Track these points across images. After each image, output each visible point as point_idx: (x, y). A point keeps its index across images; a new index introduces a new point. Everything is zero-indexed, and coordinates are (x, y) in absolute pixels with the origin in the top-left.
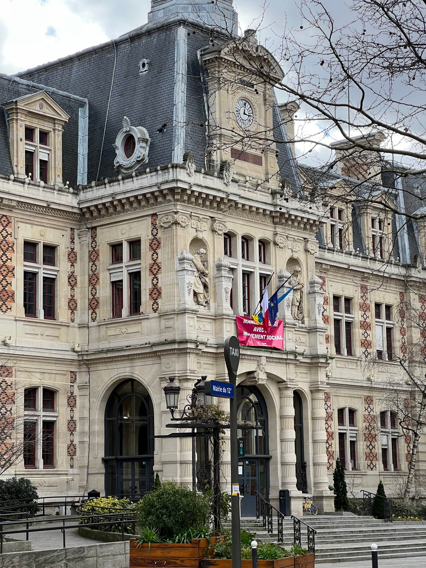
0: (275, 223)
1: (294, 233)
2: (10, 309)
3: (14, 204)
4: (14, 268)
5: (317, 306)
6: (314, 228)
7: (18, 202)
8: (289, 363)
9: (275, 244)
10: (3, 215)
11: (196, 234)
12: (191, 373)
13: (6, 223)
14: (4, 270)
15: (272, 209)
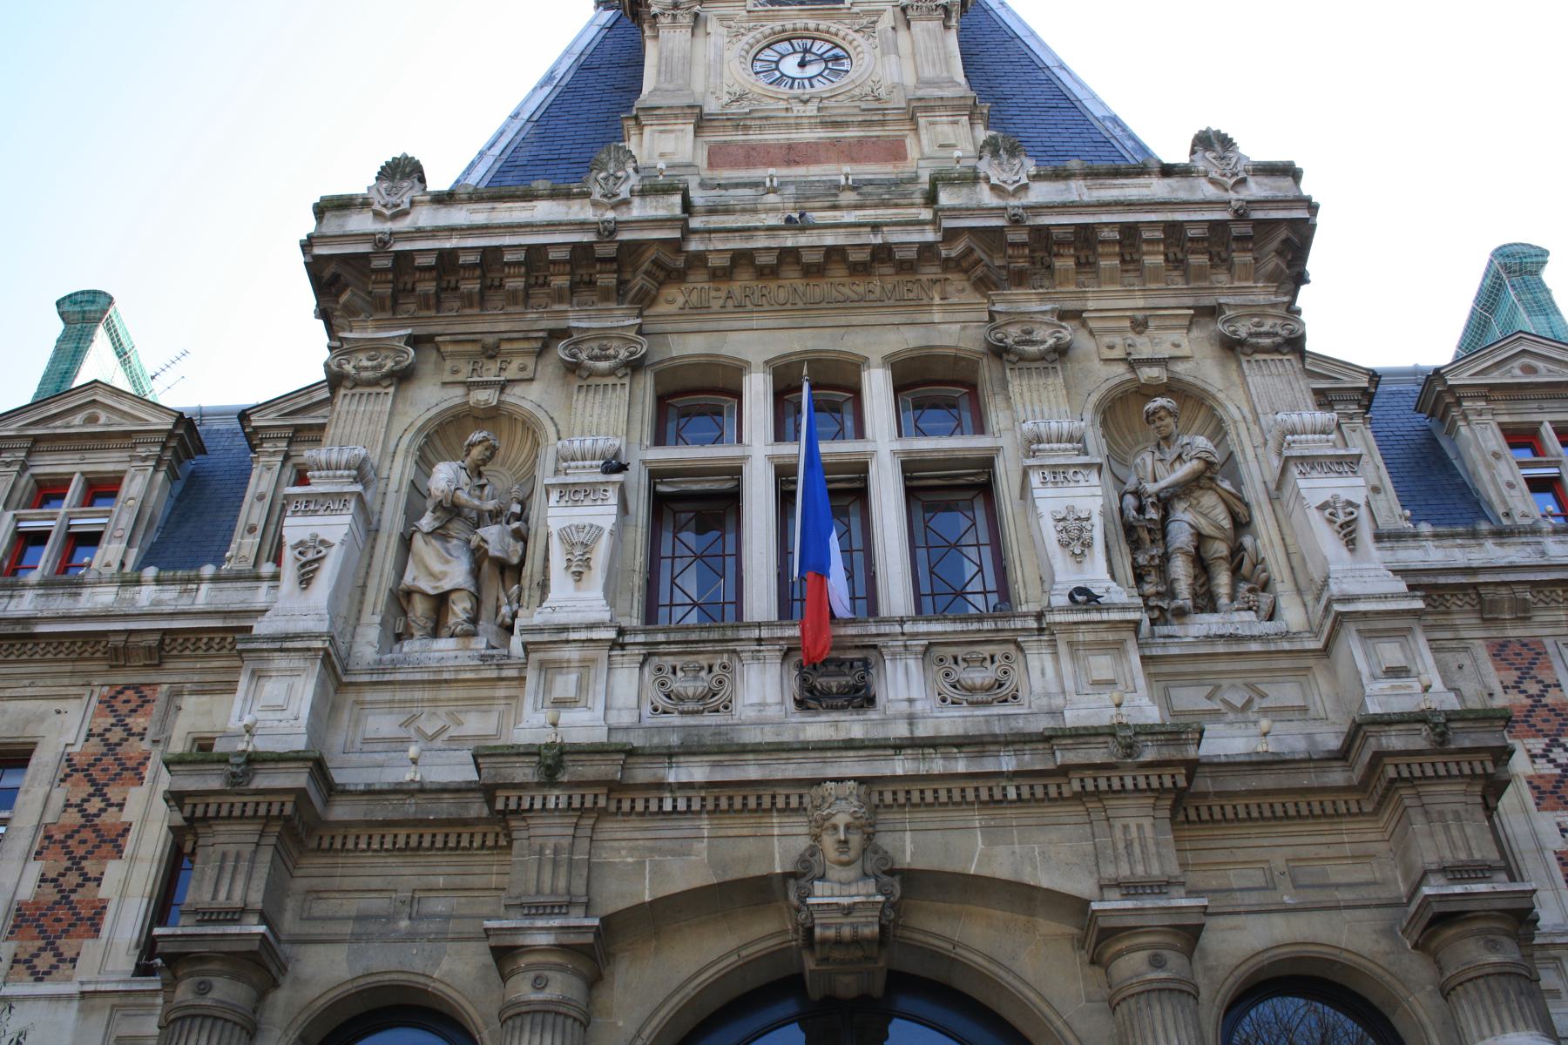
0: (984, 285)
1: (1110, 299)
2: (73, 960)
3: (152, 640)
4: (127, 830)
5: (1317, 520)
6: (1241, 258)
7: (165, 632)
8: (1097, 794)
9: (999, 352)
10: (127, 687)
11: (458, 401)
12: (201, 923)
13: (132, 705)
14: (84, 842)
15: (930, 236)
